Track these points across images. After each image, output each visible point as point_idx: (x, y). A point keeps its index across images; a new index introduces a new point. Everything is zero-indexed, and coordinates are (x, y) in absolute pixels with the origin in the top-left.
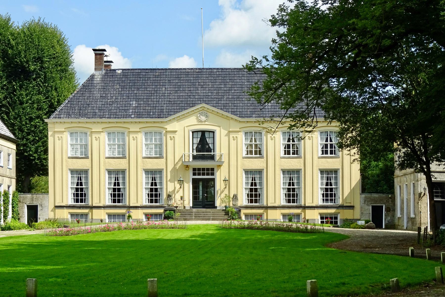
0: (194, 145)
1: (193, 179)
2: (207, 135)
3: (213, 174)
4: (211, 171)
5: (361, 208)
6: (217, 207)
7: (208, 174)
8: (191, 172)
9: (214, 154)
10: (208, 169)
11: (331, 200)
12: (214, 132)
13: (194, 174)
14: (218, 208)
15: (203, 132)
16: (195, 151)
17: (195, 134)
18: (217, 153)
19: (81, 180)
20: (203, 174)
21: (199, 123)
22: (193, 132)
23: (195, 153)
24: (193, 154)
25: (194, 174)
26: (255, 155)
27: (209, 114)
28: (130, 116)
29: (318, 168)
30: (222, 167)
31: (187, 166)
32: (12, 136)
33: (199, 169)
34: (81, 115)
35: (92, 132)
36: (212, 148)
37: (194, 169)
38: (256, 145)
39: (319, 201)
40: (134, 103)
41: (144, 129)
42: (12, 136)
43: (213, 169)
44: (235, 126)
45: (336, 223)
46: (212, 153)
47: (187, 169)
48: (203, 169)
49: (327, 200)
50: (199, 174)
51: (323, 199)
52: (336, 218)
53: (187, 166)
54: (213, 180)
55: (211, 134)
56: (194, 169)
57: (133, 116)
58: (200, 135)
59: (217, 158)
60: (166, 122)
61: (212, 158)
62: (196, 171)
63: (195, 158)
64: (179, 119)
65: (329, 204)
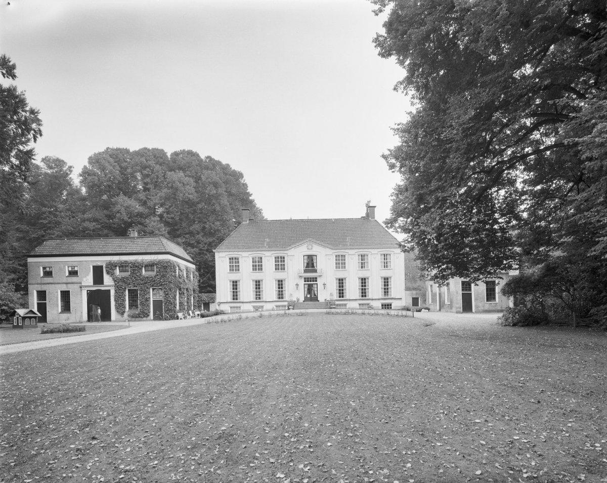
3: (316, 281)
4: (315, 279)
7: (313, 281)
8: (303, 280)
10: (313, 278)
12: (316, 256)
13: (305, 281)
20: (311, 281)
22: (304, 256)
25: (305, 281)
27: (313, 245)
31: (301, 277)
32: (192, 261)
33: (308, 278)
35: (242, 257)
40: (267, 240)
41: (274, 255)
42: (192, 261)
43: (316, 278)
44: (329, 251)
48: (311, 278)
50: (308, 281)
56: (305, 278)
61: (315, 271)
62: (306, 279)
63: (305, 271)
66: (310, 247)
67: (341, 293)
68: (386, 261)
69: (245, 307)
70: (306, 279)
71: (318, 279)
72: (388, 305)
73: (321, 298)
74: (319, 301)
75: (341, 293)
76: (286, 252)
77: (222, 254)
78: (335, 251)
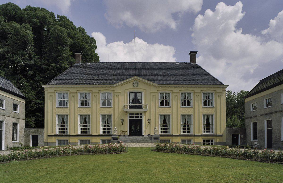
0: (130, 100)
1: (130, 120)
2: (138, 94)
3: (141, 117)
4: (140, 115)
5: (227, 135)
6: (143, 135)
7: (138, 117)
8: (128, 116)
9: (142, 105)
10: (138, 114)
11: (209, 132)
12: (142, 93)
13: (130, 117)
14: (144, 136)
15: (136, 93)
16: (130, 103)
17: (131, 94)
18: (143, 104)
19: (86, 120)
20: (136, 117)
21: (134, 88)
22: (130, 93)
23: (130, 104)
24: (130, 105)
25: (130, 117)
26: (187, 106)
27: (139, 83)
28: (93, 84)
29: (202, 113)
30: (147, 113)
31: (126, 112)
33: (133, 114)
34: (64, 83)
36: (140, 101)
37: (130, 114)
38: (166, 101)
39: (202, 132)
43: (141, 114)
44: (154, 90)
45: (212, 144)
46: (141, 104)
47: (126, 114)
48: (136, 114)
49: (207, 132)
50: (133, 117)
51: (205, 131)
52: (212, 141)
53: (126, 112)
54: (142, 120)
55: (141, 94)
56: (130, 114)
57: (95, 84)
58: (134, 94)
59: (144, 107)
60: (114, 87)
61: (140, 107)
62: (131, 115)
63: (131, 107)
64: (121, 85)
65: (208, 134)
66: (136, 85)
67: (165, 128)
68: (208, 99)
69: (72, 140)
70: (131, 115)
71: (143, 115)
72: (209, 141)
73: (145, 132)
74: (143, 136)
75: (165, 128)
76: (112, 89)
77: (50, 90)
78: (160, 89)
